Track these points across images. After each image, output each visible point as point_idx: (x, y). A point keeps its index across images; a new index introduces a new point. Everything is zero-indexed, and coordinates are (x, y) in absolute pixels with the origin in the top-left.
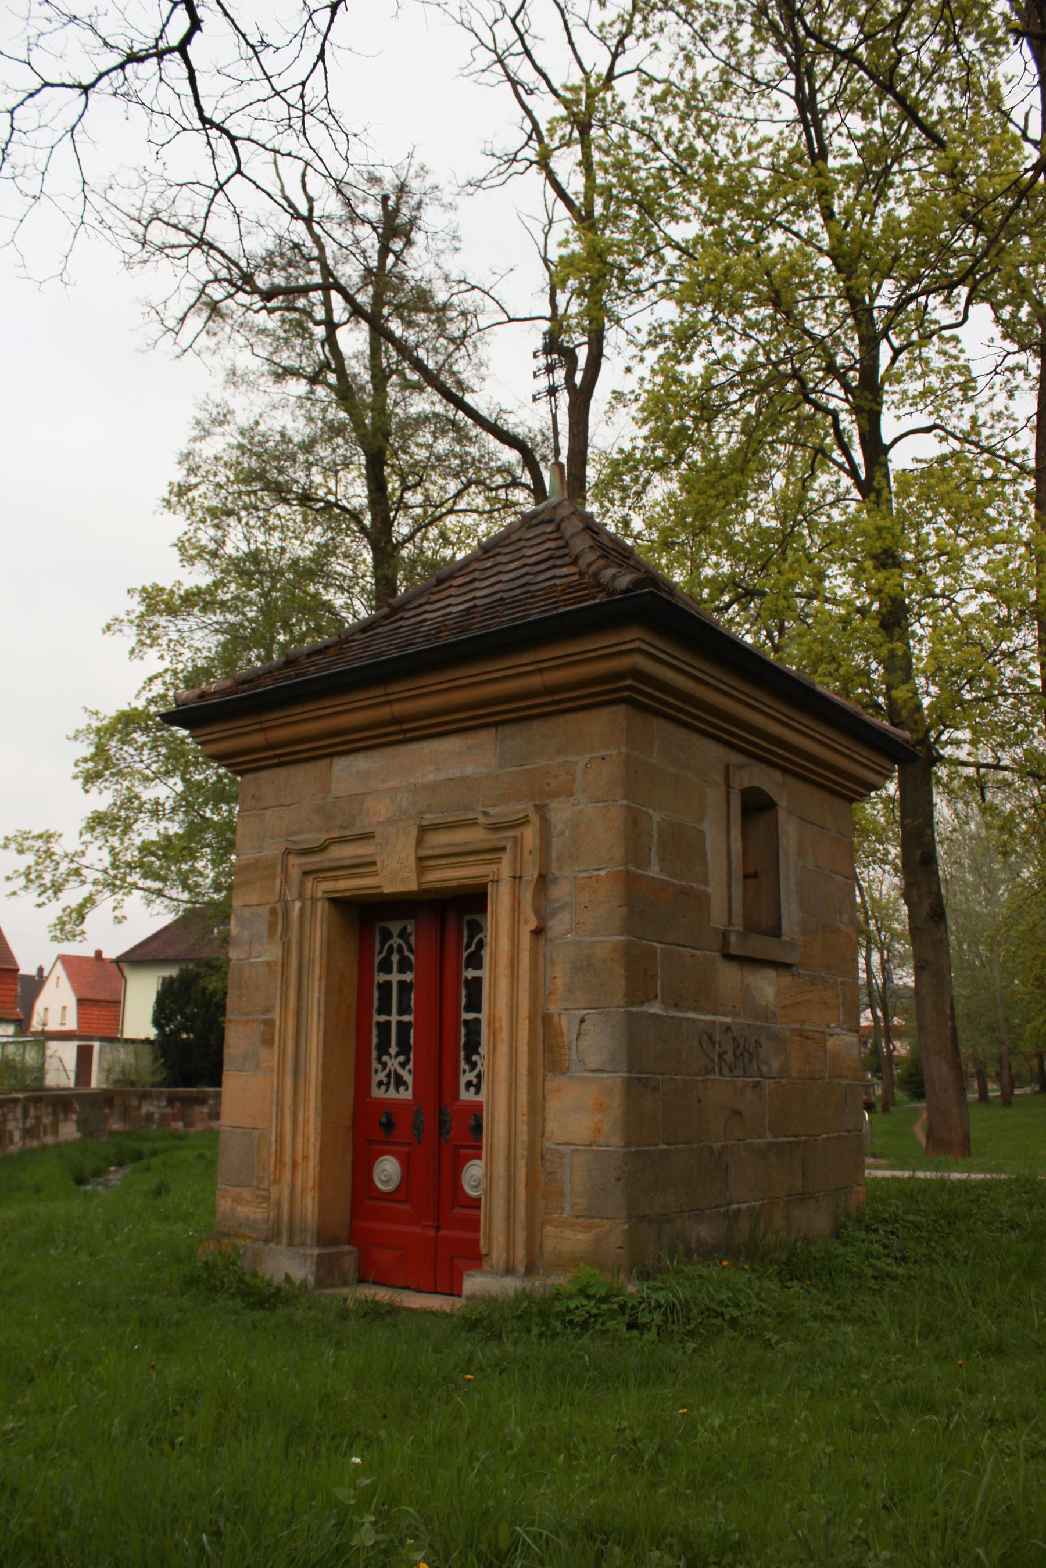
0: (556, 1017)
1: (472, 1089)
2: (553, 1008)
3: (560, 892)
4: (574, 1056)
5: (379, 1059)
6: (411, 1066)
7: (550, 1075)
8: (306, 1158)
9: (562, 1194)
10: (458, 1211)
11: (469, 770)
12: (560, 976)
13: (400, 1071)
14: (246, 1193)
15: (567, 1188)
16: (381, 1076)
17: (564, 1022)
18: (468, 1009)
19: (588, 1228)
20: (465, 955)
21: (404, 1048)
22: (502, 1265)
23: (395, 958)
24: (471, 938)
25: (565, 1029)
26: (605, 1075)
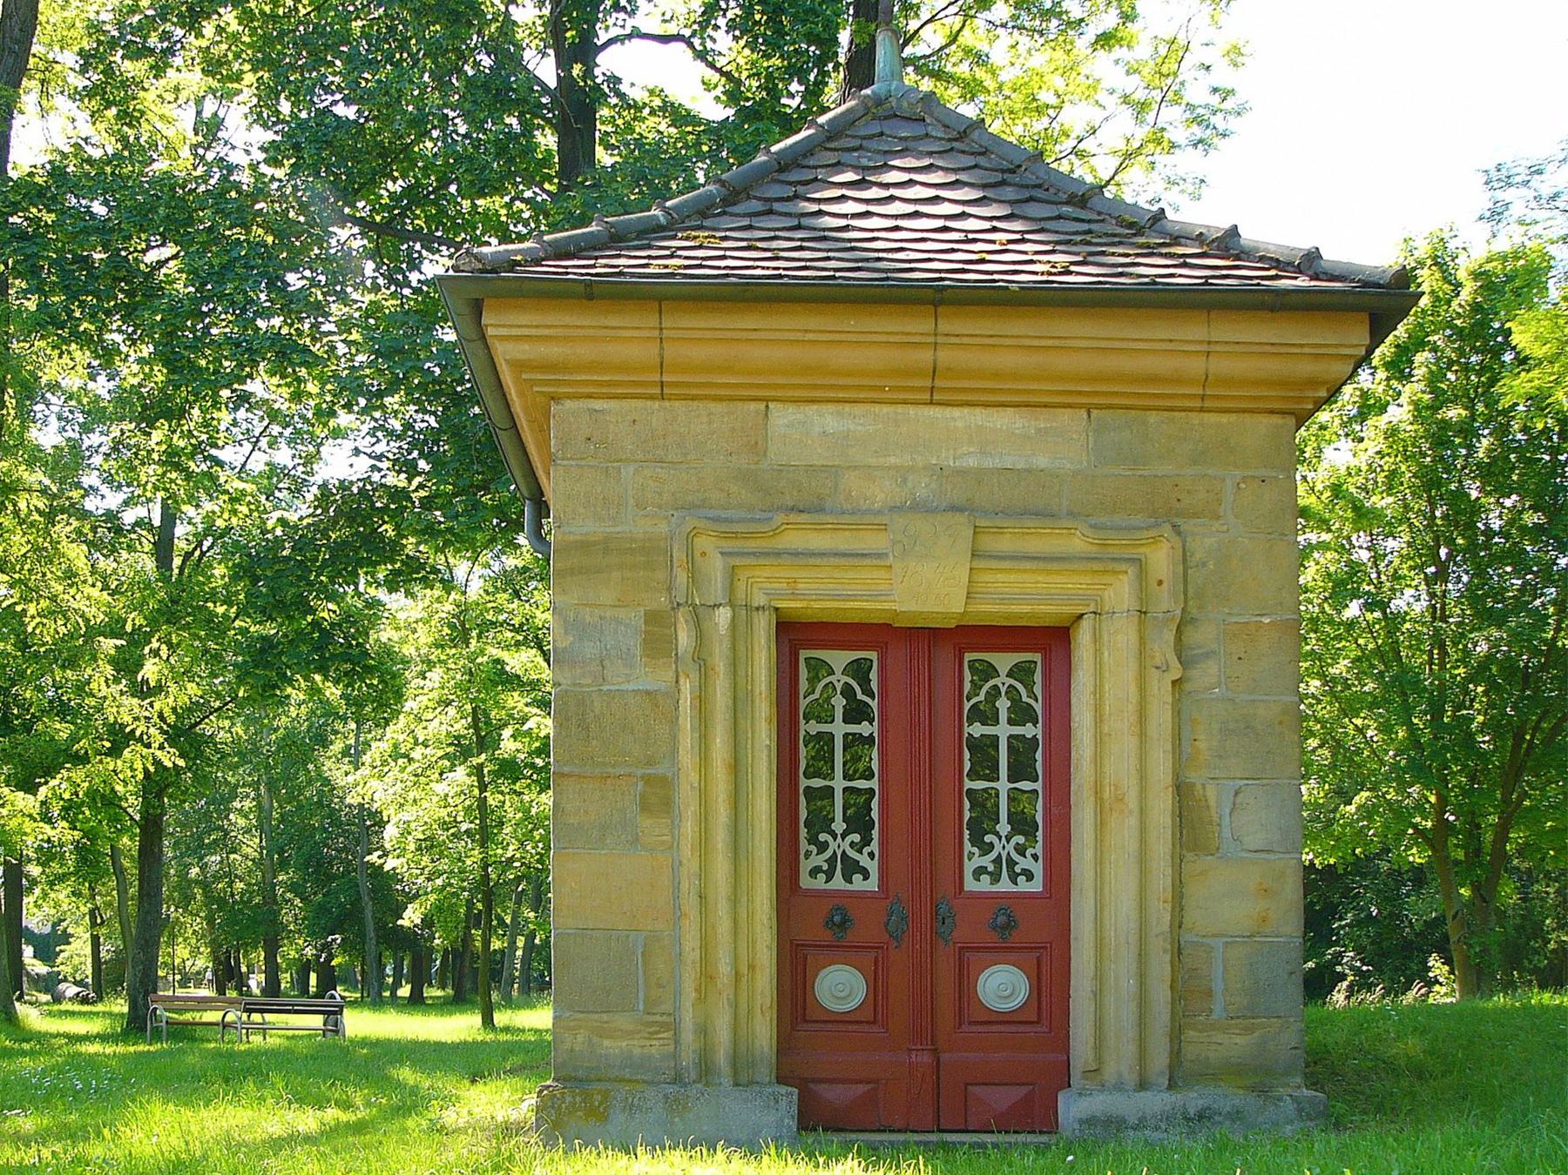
0: (1199, 787)
1: (822, 877)
2: (1193, 776)
3: (1203, 636)
4: (1226, 833)
5: (813, 840)
6: (874, 846)
7: (1189, 856)
8: (751, 967)
9: (1209, 993)
10: (805, 1026)
11: (1042, 461)
12: (1204, 744)
13: (852, 853)
14: (622, 1021)
15: (1218, 986)
16: (820, 860)
17: (1211, 793)
18: (974, 775)
19: (1248, 1030)
20: (967, 706)
21: (859, 822)
22: (1131, 1079)
23: (1003, 704)
24: (813, 681)
25: (1212, 803)
26: (1271, 856)
